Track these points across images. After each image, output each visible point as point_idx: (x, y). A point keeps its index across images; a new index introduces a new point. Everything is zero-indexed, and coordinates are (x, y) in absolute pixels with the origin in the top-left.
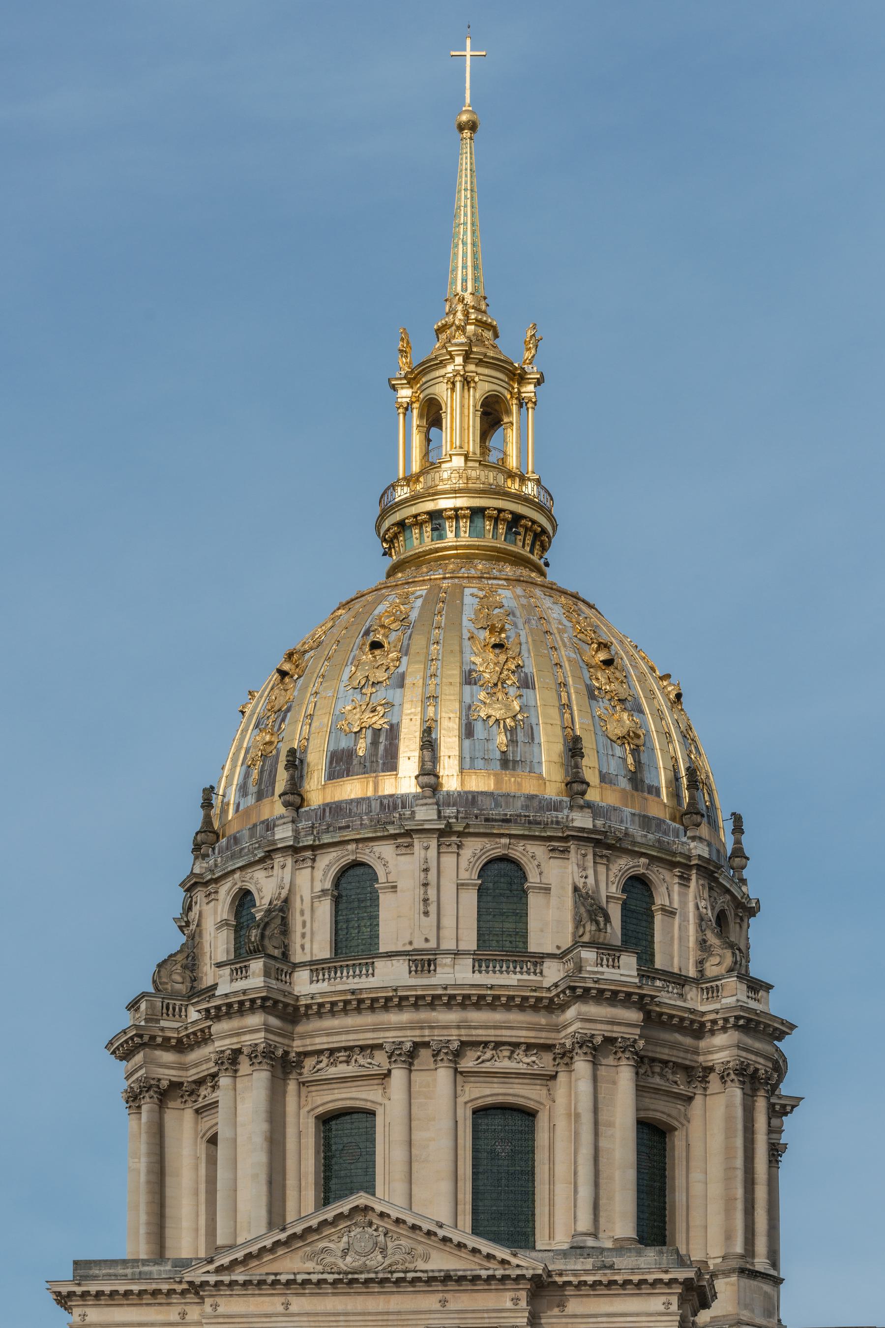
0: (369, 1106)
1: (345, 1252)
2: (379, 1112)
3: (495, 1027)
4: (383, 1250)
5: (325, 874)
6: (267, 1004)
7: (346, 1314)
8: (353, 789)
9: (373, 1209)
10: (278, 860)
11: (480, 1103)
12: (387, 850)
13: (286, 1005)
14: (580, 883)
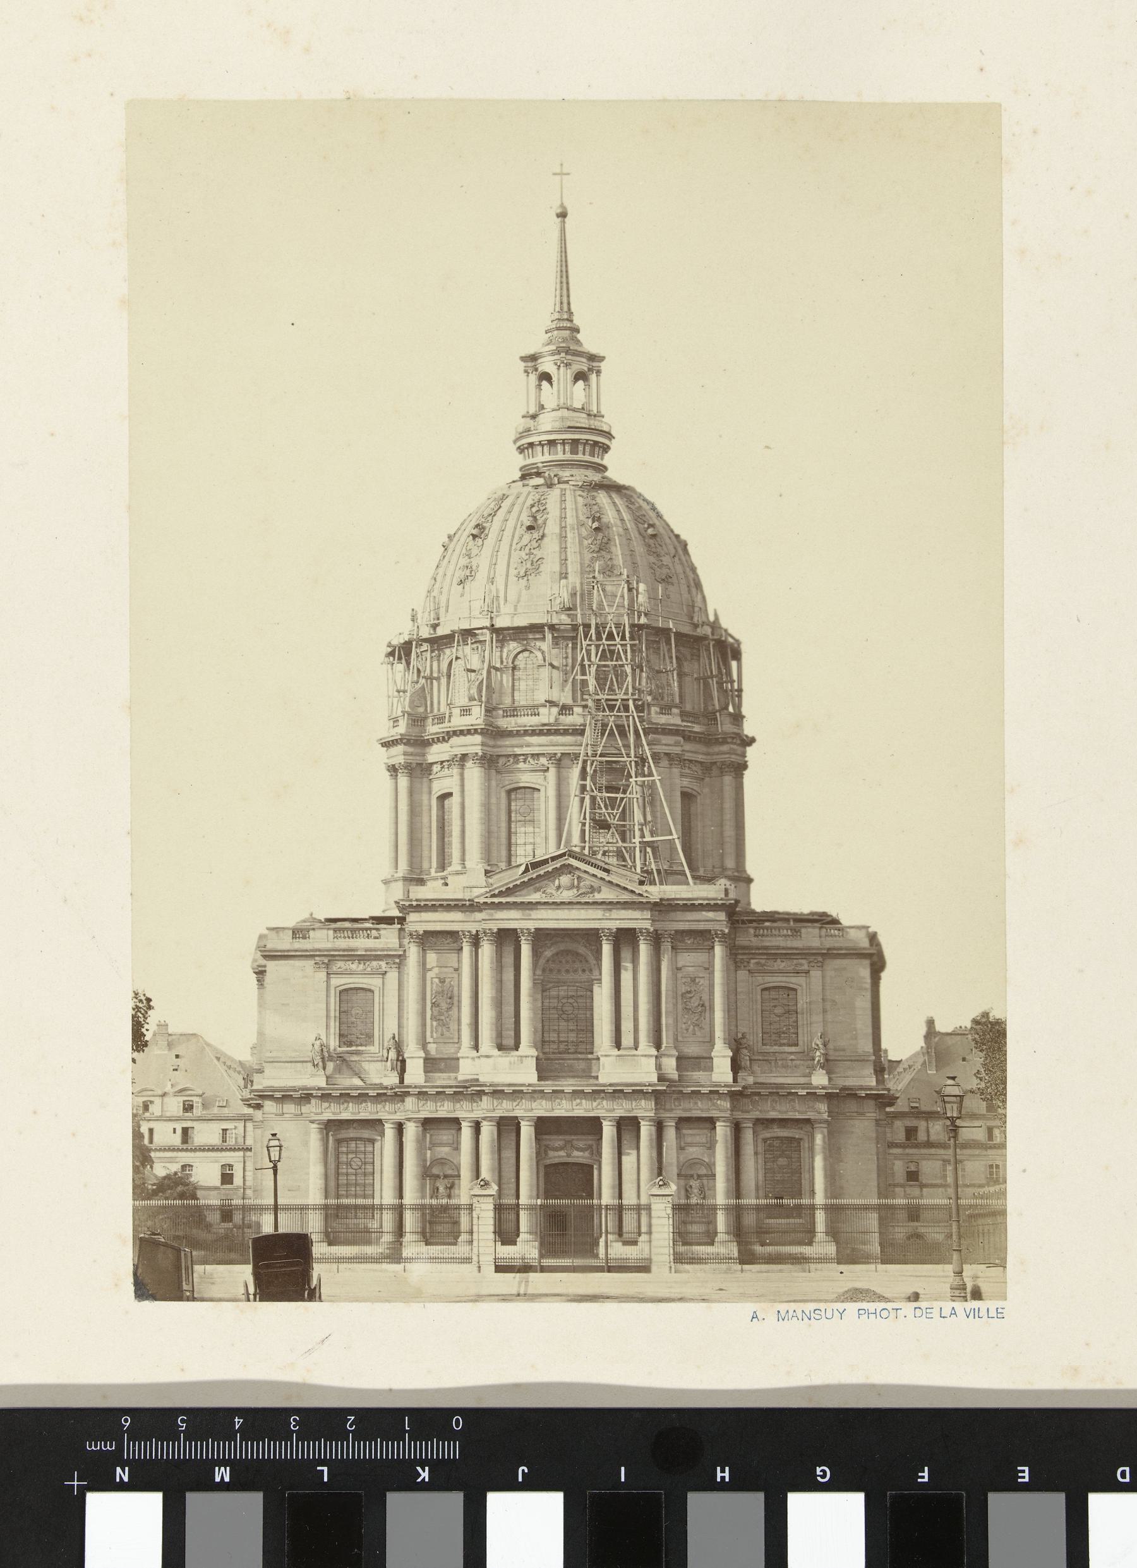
2: (543, 789)
4: (578, 888)
6: (483, 732)
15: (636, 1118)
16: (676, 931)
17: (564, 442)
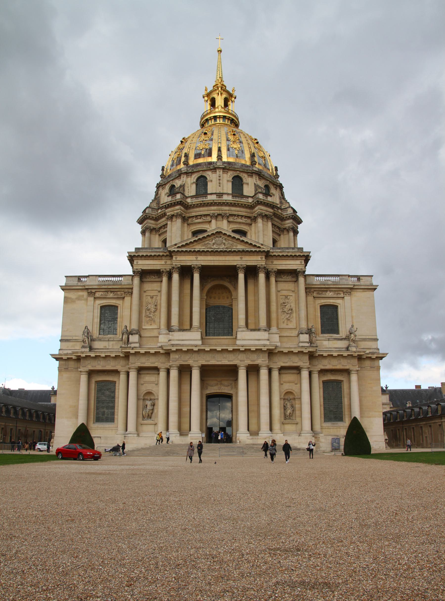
0: (205, 229)
1: (214, 244)
3: (238, 211)
4: (224, 244)
5: (194, 178)
7: (214, 261)
8: (201, 161)
9: (221, 232)
10: (182, 176)
11: (234, 229)
12: (209, 173)
13: (186, 204)
14: (256, 183)
15: (258, 365)
16: (278, 270)
17: (220, 117)
